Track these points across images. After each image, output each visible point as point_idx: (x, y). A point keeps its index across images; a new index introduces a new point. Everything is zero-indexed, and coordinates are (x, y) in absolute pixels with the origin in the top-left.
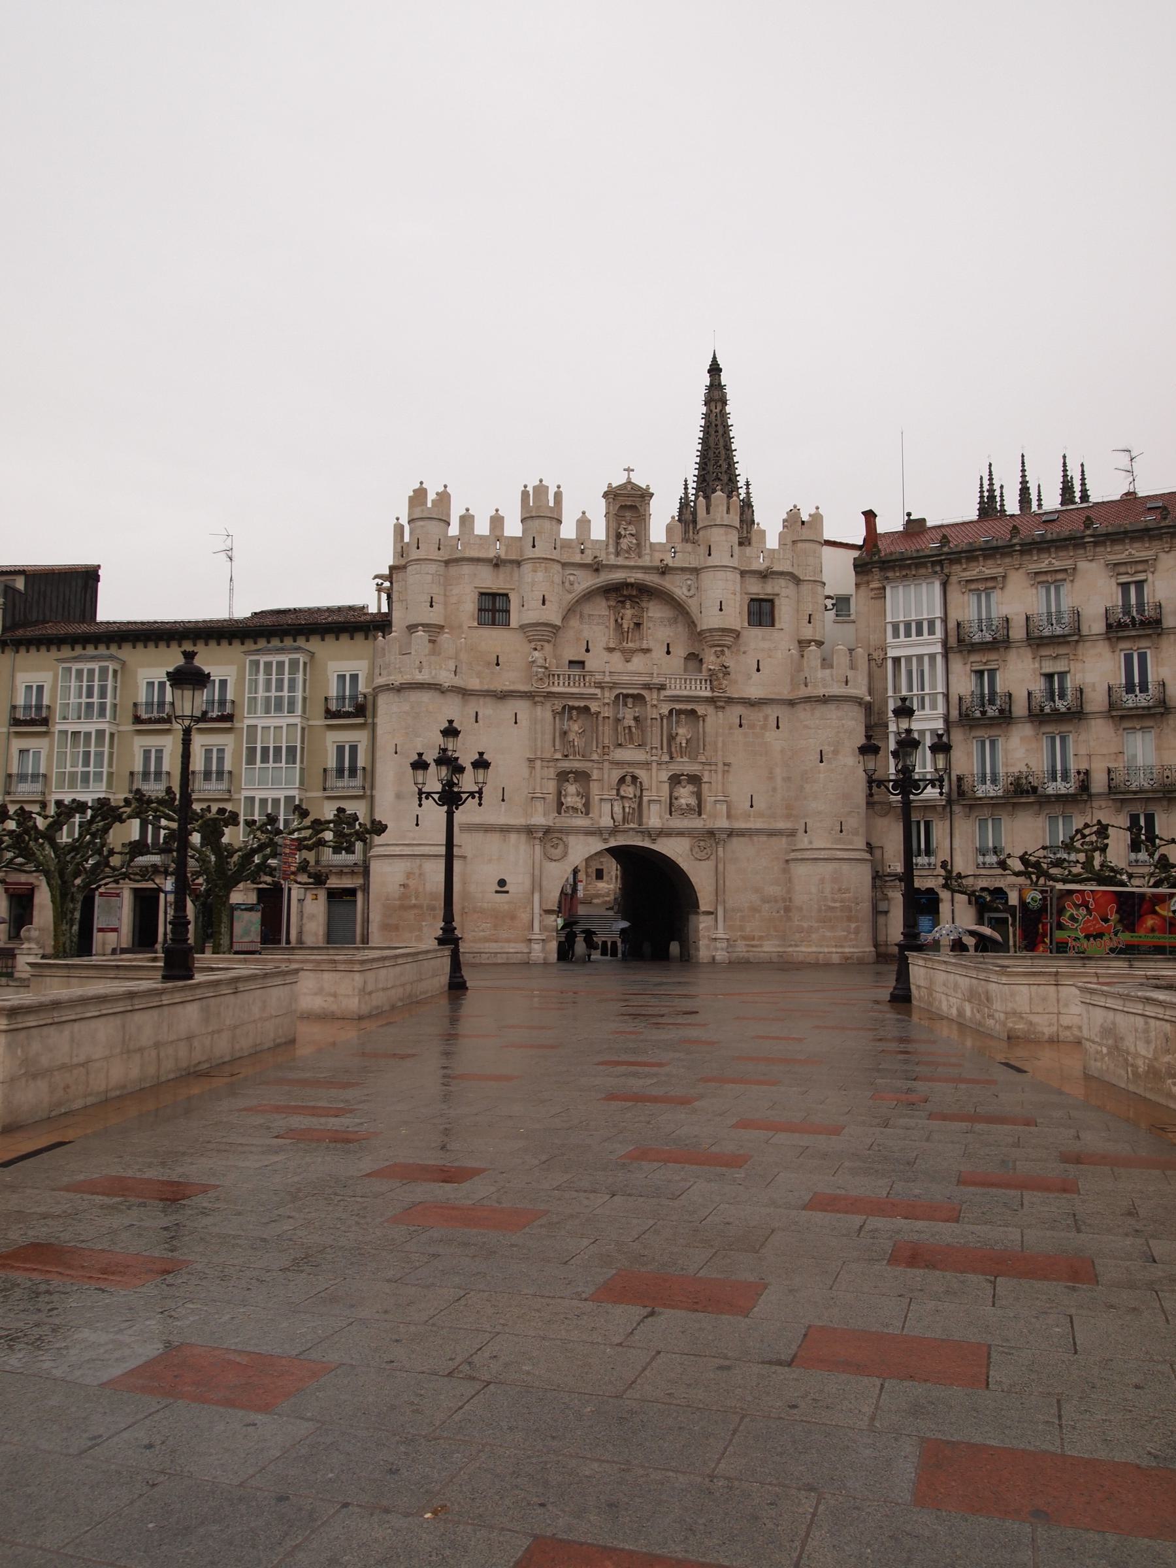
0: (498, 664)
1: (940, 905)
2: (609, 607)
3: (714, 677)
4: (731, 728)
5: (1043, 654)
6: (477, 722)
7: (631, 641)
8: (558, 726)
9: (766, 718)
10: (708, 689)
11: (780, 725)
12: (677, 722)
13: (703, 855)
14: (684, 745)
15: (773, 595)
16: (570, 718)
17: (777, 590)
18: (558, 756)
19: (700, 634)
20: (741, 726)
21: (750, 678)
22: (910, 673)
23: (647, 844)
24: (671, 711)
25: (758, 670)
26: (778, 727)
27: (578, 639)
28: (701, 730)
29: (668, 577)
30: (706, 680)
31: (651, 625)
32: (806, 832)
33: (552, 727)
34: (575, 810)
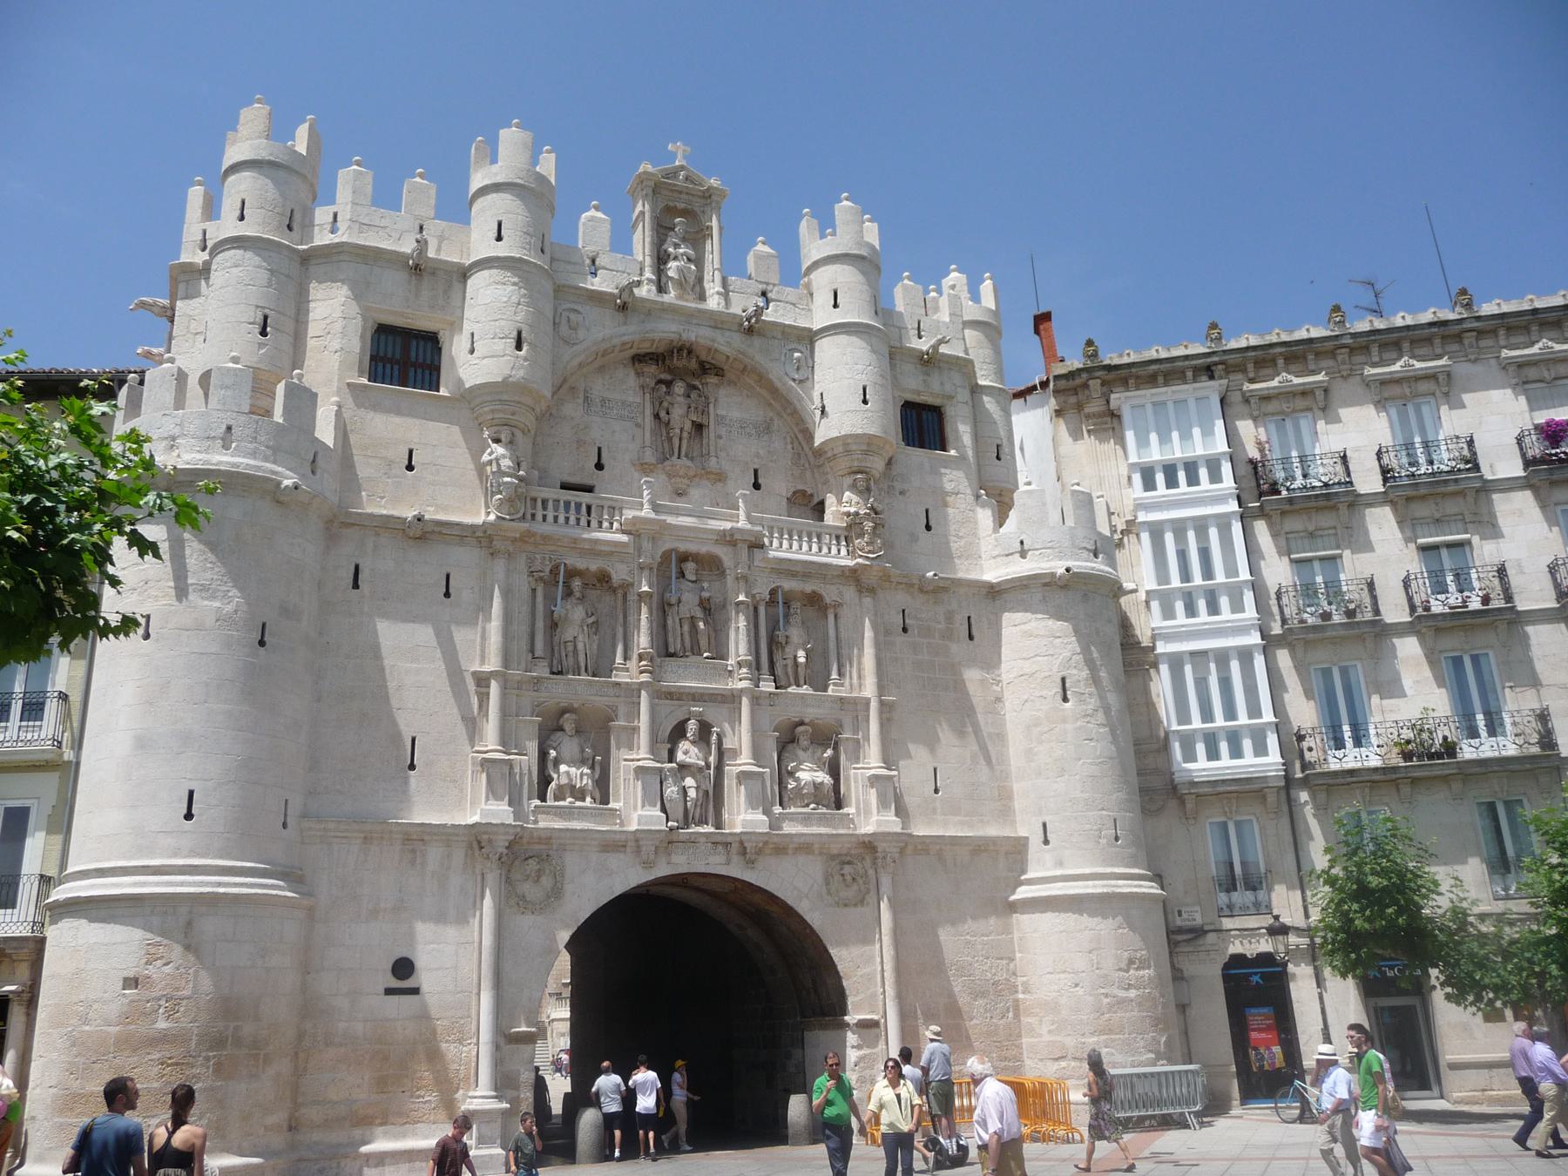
0: (410, 467)
1: (1292, 986)
2: (643, 387)
3: (856, 529)
4: (887, 633)
5: (1418, 515)
6: (356, 586)
7: (686, 456)
8: (540, 607)
9: (949, 617)
10: (844, 551)
11: (974, 632)
12: (786, 616)
13: (850, 893)
14: (802, 660)
15: (943, 396)
16: (568, 593)
17: (948, 388)
18: (542, 671)
19: (819, 453)
20: (905, 630)
21: (917, 540)
22: (1182, 555)
23: (736, 871)
24: (773, 592)
25: (928, 528)
26: (971, 637)
27: (580, 443)
28: (832, 632)
29: (757, 341)
30: (838, 538)
31: (723, 431)
32: (1046, 842)
33: (526, 609)
34: (580, 794)
